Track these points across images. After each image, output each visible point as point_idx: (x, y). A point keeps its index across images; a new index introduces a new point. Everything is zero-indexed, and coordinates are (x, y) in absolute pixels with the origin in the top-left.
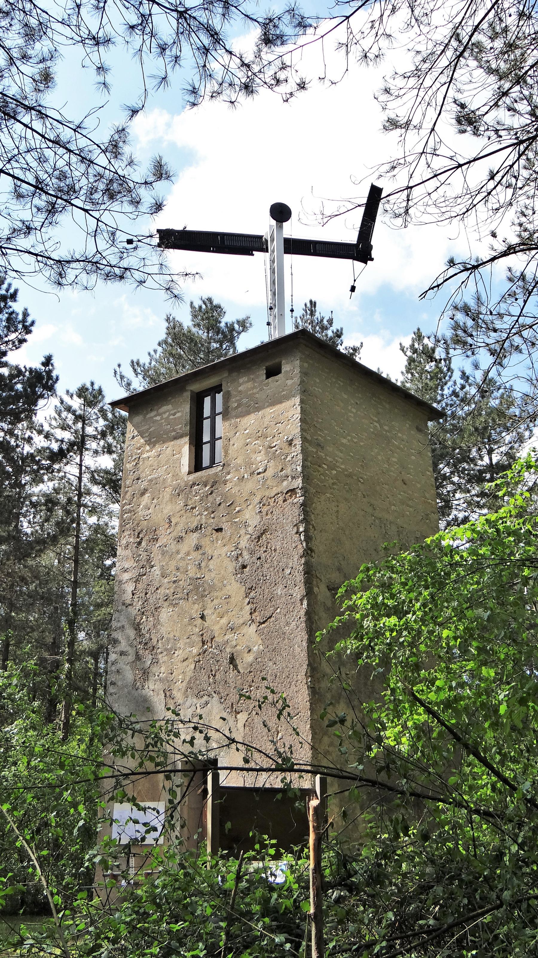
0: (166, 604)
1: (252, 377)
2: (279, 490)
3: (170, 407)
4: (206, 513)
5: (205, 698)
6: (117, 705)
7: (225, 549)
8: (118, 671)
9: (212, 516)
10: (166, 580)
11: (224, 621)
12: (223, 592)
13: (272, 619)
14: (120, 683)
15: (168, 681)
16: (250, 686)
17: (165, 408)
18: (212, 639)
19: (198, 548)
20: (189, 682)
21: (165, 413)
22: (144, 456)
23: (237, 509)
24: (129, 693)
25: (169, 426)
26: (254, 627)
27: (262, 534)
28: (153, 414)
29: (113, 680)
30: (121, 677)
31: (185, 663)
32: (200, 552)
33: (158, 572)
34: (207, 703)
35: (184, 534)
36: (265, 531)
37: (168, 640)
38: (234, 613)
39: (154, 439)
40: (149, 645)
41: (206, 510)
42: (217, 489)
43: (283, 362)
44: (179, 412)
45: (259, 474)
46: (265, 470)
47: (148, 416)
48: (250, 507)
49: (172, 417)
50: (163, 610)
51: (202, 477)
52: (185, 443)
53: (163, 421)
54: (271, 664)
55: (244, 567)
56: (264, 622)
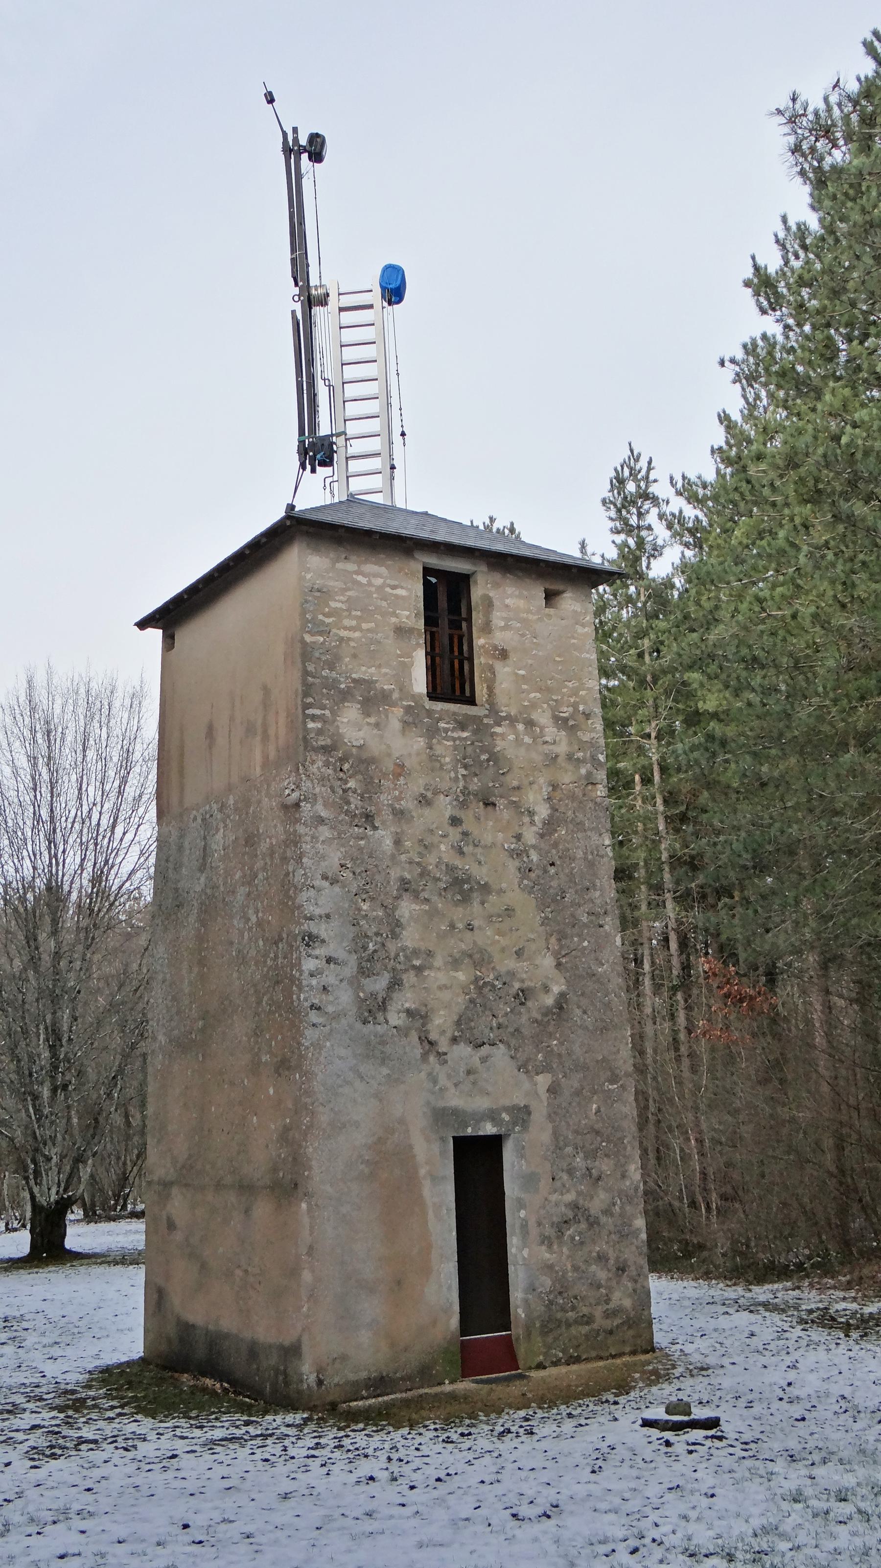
0: (406, 896)
1: (525, 593)
3: (383, 570)
4: (465, 772)
5: (486, 1049)
6: (328, 1044)
8: (325, 988)
10: (403, 858)
14: (330, 1009)
15: (422, 1017)
19: (455, 821)
20: (458, 1023)
21: (376, 575)
23: (515, 783)
24: (351, 1027)
25: (384, 604)
28: (351, 567)
29: (316, 1001)
30: (331, 998)
32: (460, 830)
33: (388, 842)
35: (429, 794)
37: (416, 953)
39: (359, 613)
40: (382, 954)
41: (465, 767)
42: (481, 741)
43: (567, 595)
44: (402, 588)
45: (546, 743)
46: (555, 742)
47: (340, 566)
48: (535, 787)
49: (388, 590)
51: (454, 714)
52: (418, 644)
53: (373, 589)
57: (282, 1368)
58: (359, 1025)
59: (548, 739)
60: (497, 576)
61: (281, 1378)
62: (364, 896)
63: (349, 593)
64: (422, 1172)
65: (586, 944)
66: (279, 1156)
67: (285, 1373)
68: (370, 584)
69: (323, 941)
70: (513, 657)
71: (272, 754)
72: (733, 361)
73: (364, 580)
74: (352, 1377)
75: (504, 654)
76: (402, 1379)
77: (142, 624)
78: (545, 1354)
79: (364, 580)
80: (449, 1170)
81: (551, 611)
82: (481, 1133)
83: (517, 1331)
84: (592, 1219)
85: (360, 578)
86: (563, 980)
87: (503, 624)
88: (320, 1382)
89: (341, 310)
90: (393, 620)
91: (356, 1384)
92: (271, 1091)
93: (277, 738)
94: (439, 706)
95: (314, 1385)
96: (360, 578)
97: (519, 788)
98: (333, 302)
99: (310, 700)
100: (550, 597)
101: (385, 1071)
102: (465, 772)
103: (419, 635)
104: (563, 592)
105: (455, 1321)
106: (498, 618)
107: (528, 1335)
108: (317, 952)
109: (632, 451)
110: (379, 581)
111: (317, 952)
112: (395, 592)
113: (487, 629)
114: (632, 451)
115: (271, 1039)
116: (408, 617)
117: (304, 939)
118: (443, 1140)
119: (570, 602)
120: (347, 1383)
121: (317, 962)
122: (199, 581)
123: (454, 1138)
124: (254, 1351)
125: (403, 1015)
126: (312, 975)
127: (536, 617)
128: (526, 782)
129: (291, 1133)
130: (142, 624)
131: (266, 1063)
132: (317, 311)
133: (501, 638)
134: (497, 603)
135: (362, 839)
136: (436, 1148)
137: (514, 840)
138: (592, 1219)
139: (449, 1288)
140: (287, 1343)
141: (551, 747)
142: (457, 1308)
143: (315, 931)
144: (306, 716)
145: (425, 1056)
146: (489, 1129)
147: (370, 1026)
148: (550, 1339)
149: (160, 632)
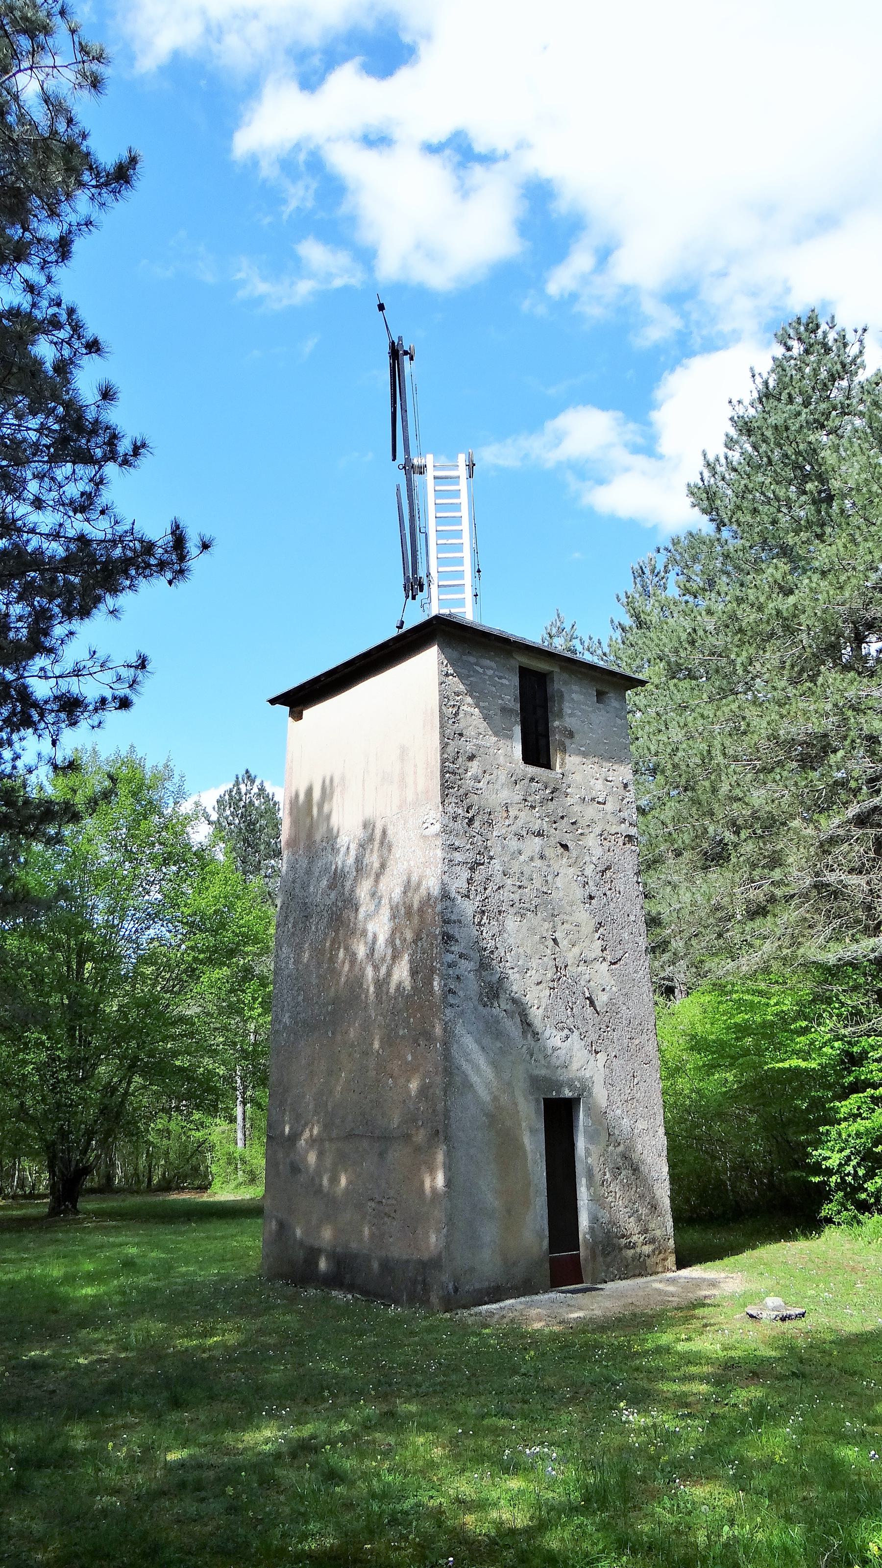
0: (512, 911)
1: (584, 691)
2: (618, 830)
3: (493, 664)
5: (566, 1031)
7: (571, 870)
8: (458, 978)
9: (554, 826)
10: (509, 882)
11: (576, 950)
12: (573, 918)
13: (622, 962)
14: (461, 993)
16: (608, 1027)
17: (487, 662)
18: (566, 967)
22: (465, 708)
26: (605, 965)
27: (606, 869)
28: (472, 659)
31: (540, 987)
34: (567, 1037)
36: (608, 868)
38: (585, 944)
45: (599, 803)
47: (464, 658)
49: (496, 679)
50: (509, 916)
54: (625, 1008)
55: (591, 898)
56: (615, 963)
57: (419, 1278)
58: (481, 1008)
59: (600, 800)
60: (565, 676)
61: (419, 1287)
62: (483, 908)
63: (471, 679)
64: (524, 1124)
65: (627, 955)
66: (418, 1109)
67: (424, 1282)
68: (484, 673)
69: (457, 941)
70: (577, 737)
71: (410, 797)
72: (666, 549)
73: (481, 671)
74: (477, 1286)
75: (571, 735)
76: (512, 1288)
77: (273, 701)
78: (606, 1271)
79: (481, 671)
80: (541, 1126)
81: (601, 706)
82: (561, 1096)
83: (583, 1252)
84: (634, 1167)
85: (478, 668)
86: (613, 982)
87: (570, 712)
88: (456, 1290)
89: (435, 478)
90: (500, 702)
91: (480, 1291)
92: (410, 1058)
93: (415, 784)
94: (532, 770)
95: (452, 1291)
96: (478, 668)
97: (581, 834)
98: (430, 473)
99: (446, 756)
100: (600, 696)
101: (499, 1044)
102: (547, 819)
103: (517, 715)
104: (607, 693)
105: (546, 1243)
106: (567, 708)
107: (594, 1256)
108: (453, 948)
109: (558, 615)
110: (490, 672)
111: (453, 948)
112: (500, 681)
113: (560, 715)
114: (558, 615)
115: (409, 1017)
116: (509, 701)
117: (443, 938)
118: (537, 1100)
119: (613, 701)
120: (475, 1290)
121: (453, 956)
122: (337, 668)
123: (545, 1099)
124: (387, 1266)
125: (510, 1002)
126: (450, 967)
127: (590, 709)
128: (586, 831)
129: (431, 1091)
130: (273, 701)
131: (403, 1037)
132: (416, 477)
133: (570, 722)
134: (566, 696)
135: (483, 864)
136: (533, 1105)
137: (580, 874)
138: (634, 1167)
139: (542, 1217)
140: (426, 1257)
141: (602, 806)
142: (547, 1233)
143: (451, 932)
144: (443, 767)
145: (524, 1032)
146: (567, 1093)
147: (489, 1008)
148: (609, 1259)
149: (288, 708)
